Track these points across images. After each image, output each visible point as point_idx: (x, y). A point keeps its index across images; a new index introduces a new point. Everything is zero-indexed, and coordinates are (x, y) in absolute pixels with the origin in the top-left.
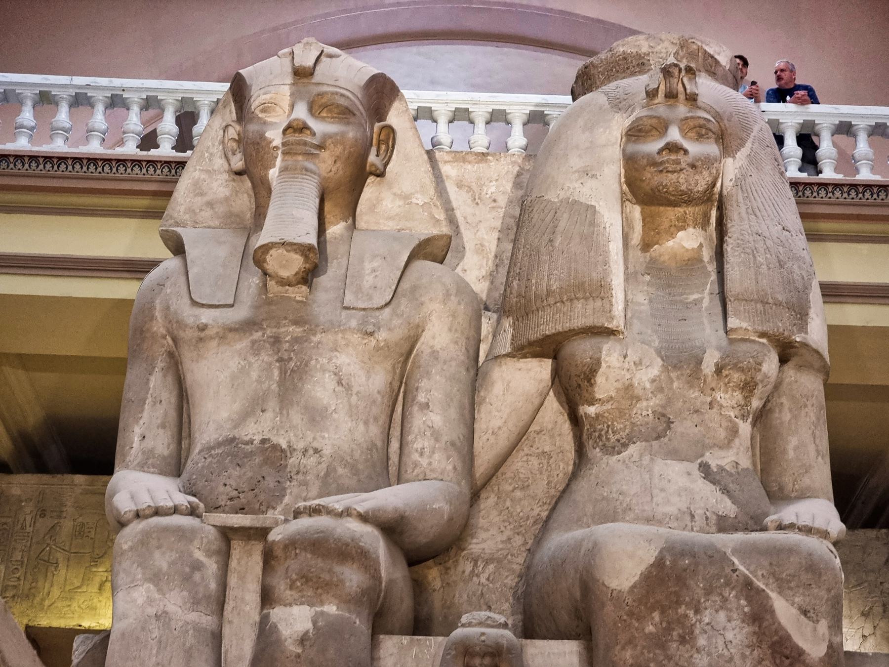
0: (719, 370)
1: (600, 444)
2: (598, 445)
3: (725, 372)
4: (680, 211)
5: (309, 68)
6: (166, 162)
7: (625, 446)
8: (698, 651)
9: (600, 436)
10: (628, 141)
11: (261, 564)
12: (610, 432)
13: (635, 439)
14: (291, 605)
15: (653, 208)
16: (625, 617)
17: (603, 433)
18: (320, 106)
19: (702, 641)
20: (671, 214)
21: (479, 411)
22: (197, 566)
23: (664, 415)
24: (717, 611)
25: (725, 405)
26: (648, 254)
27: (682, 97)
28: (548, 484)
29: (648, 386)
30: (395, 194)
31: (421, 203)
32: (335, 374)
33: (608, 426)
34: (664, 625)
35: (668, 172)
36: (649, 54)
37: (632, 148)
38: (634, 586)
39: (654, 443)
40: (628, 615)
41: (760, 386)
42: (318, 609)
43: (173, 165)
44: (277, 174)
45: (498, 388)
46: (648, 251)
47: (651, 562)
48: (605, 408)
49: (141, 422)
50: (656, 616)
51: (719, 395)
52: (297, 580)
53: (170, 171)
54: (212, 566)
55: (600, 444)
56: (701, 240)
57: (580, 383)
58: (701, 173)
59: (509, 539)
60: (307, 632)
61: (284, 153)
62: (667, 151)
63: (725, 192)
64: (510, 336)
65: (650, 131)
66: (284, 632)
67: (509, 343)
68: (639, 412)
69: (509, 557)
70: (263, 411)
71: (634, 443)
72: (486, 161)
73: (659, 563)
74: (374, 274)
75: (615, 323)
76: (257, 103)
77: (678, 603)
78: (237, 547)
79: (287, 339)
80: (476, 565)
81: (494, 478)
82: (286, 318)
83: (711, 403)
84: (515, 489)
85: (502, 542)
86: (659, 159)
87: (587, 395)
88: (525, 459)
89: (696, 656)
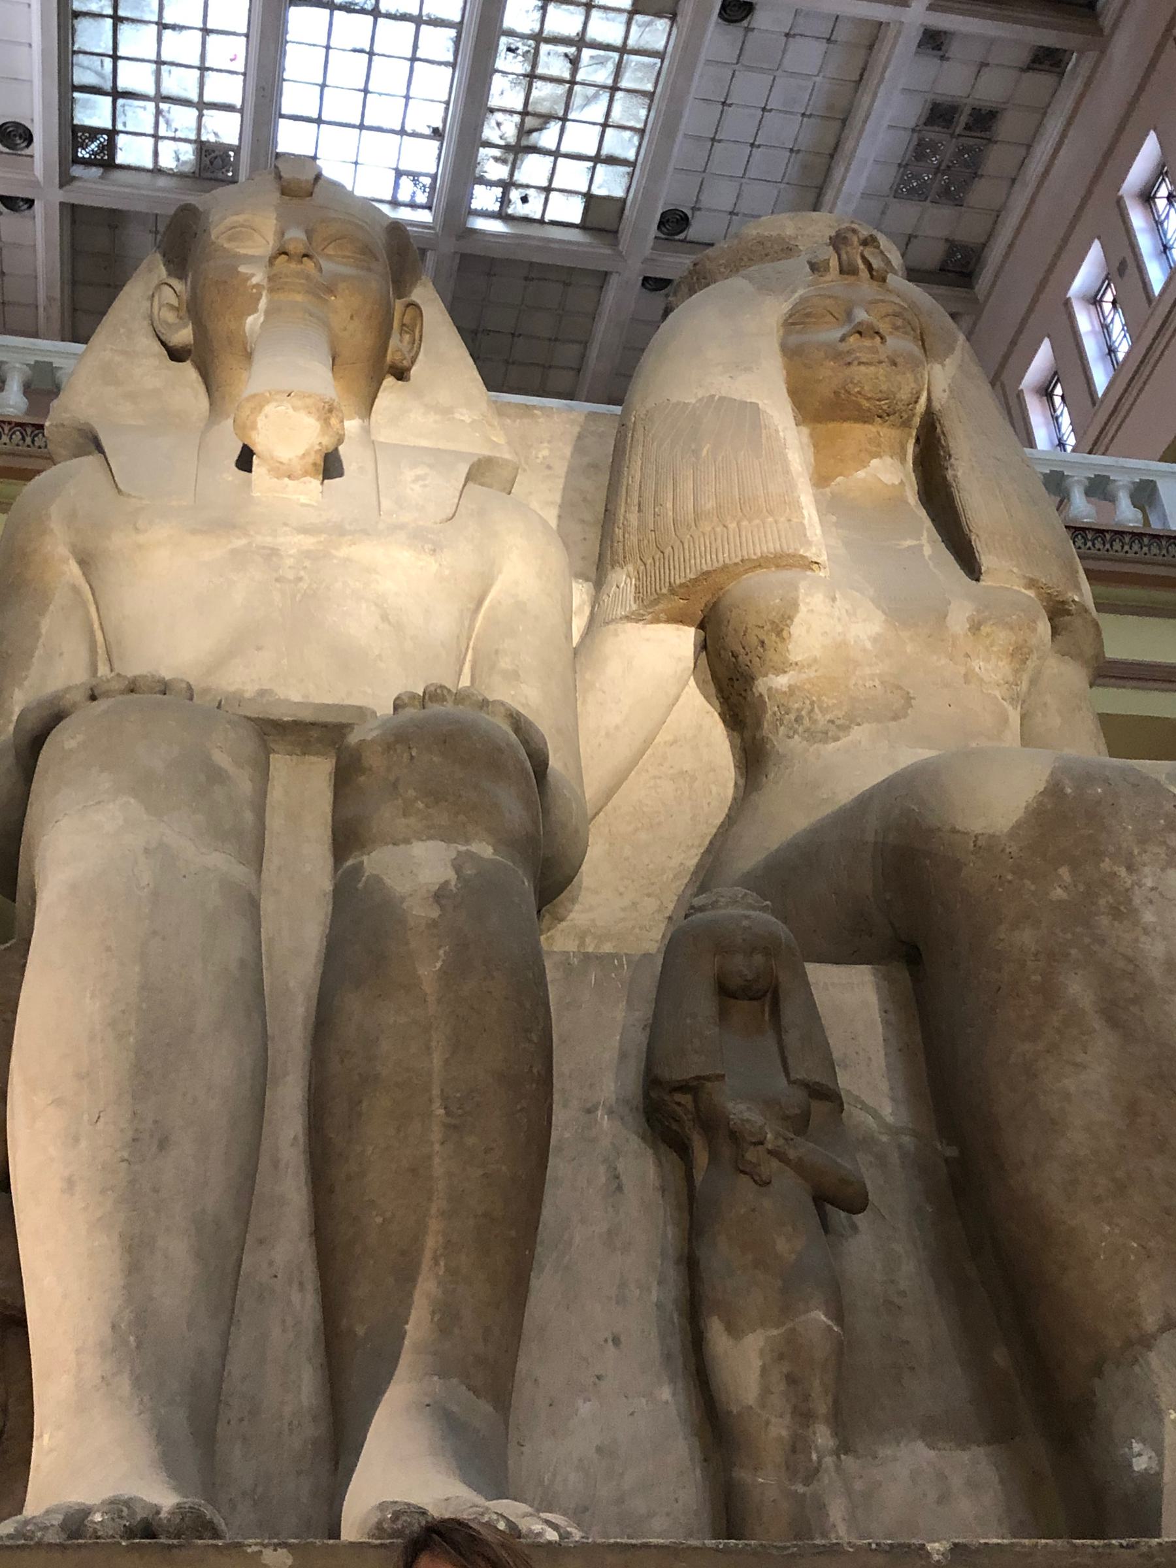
0: (975, 627)
1: (801, 729)
2: (795, 732)
3: (985, 629)
4: (871, 429)
5: (307, 181)
6: (18, 424)
7: (845, 728)
8: (1146, 932)
9: (798, 720)
10: (787, 333)
11: (329, 795)
12: (816, 709)
13: (859, 720)
14: (407, 841)
15: (831, 425)
16: (1010, 877)
17: (803, 713)
18: (324, 240)
19: (1148, 917)
20: (858, 432)
21: (584, 702)
22: (216, 776)
23: (899, 687)
24: (1163, 870)
25: (986, 679)
26: (828, 490)
27: (864, 273)
28: (693, 818)
29: (869, 645)
30: (426, 405)
31: (468, 421)
32: (376, 605)
33: (812, 703)
34: (1082, 888)
35: (860, 363)
36: (796, 238)
37: (794, 340)
38: (1018, 825)
39: (892, 724)
40: (1014, 873)
41: (1035, 656)
42: (462, 848)
43: (29, 430)
44: (262, 319)
45: (614, 668)
46: (828, 485)
47: (1042, 789)
48: (804, 676)
49: (26, 683)
50: (1064, 871)
51: (978, 665)
52: (416, 799)
53: (23, 439)
54: (244, 784)
55: (801, 729)
56: (902, 476)
57: (764, 637)
58: (904, 373)
59: (634, 904)
60: (447, 883)
61: (271, 290)
62: (857, 335)
63: (936, 405)
64: (631, 590)
65: (823, 316)
66: (398, 889)
67: (631, 597)
68: (860, 682)
69: (637, 930)
70: (259, 648)
71: (859, 725)
72: (533, 416)
73: (1054, 790)
74: (421, 483)
75: (814, 550)
76: (222, 227)
77: (1098, 855)
78: (281, 764)
79: (291, 552)
80: (582, 943)
81: (601, 814)
82: (285, 524)
83: (966, 676)
84: (636, 830)
85: (624, 909)
86: (843, 347)
87: (776, 658)
88: (652, 783)
89: (1143, 938)
